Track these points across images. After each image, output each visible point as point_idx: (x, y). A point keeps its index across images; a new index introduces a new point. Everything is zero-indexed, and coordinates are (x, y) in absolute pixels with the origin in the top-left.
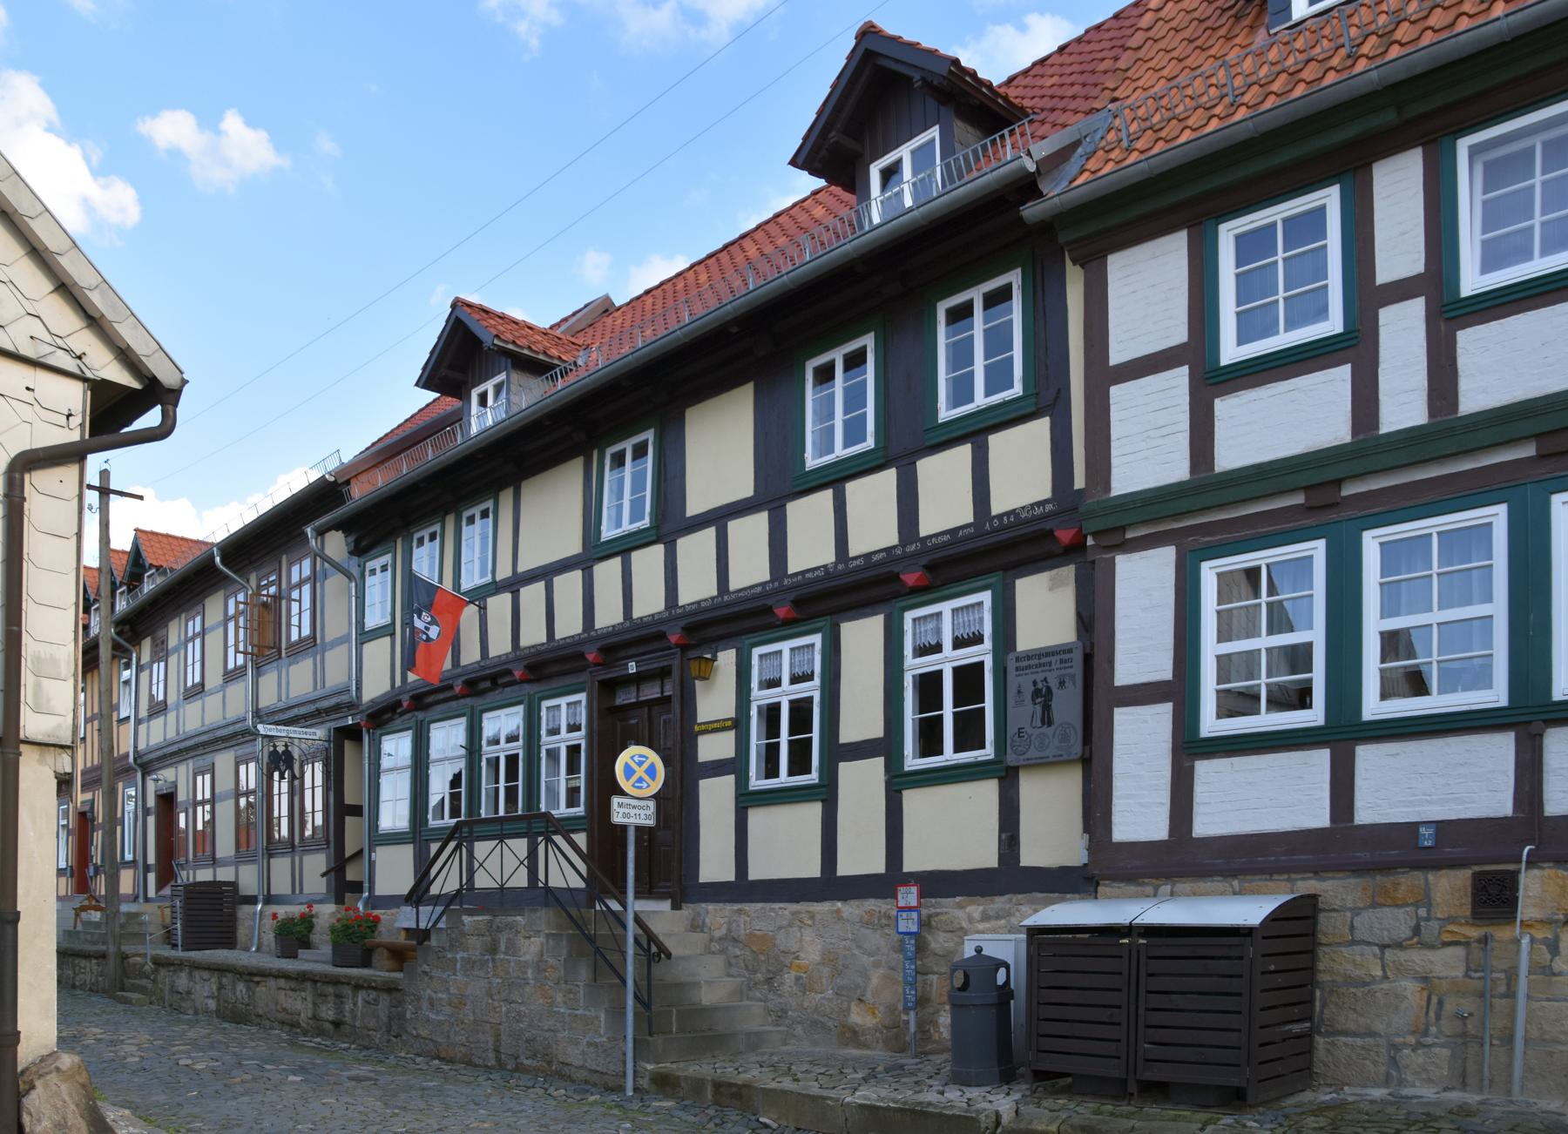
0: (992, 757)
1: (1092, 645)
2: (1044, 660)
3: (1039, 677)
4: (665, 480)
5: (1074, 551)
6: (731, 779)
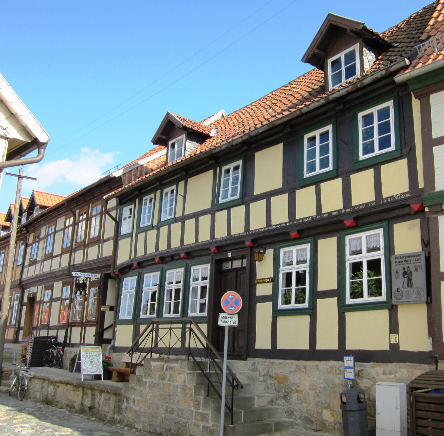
0: (385, 300)
1: (429, 253)
2: (407, 259)
3: (406, 266)
4: (246, 181)
5: (420, 213)
6: (270, 304)
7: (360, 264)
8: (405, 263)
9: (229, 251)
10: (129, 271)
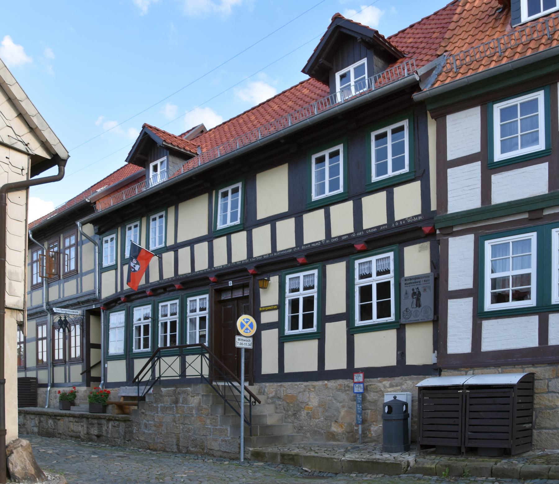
0: (394, 320)
1: (438, 275)
2: (417, 280)
3: (415, 287)
4: (247, 204)
5: (430, 236)
6: (276, 330)
7: (370, 287)
8: (415, 284)
9: (230, 279)
10: (115, 306)
